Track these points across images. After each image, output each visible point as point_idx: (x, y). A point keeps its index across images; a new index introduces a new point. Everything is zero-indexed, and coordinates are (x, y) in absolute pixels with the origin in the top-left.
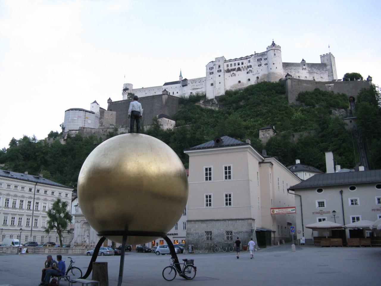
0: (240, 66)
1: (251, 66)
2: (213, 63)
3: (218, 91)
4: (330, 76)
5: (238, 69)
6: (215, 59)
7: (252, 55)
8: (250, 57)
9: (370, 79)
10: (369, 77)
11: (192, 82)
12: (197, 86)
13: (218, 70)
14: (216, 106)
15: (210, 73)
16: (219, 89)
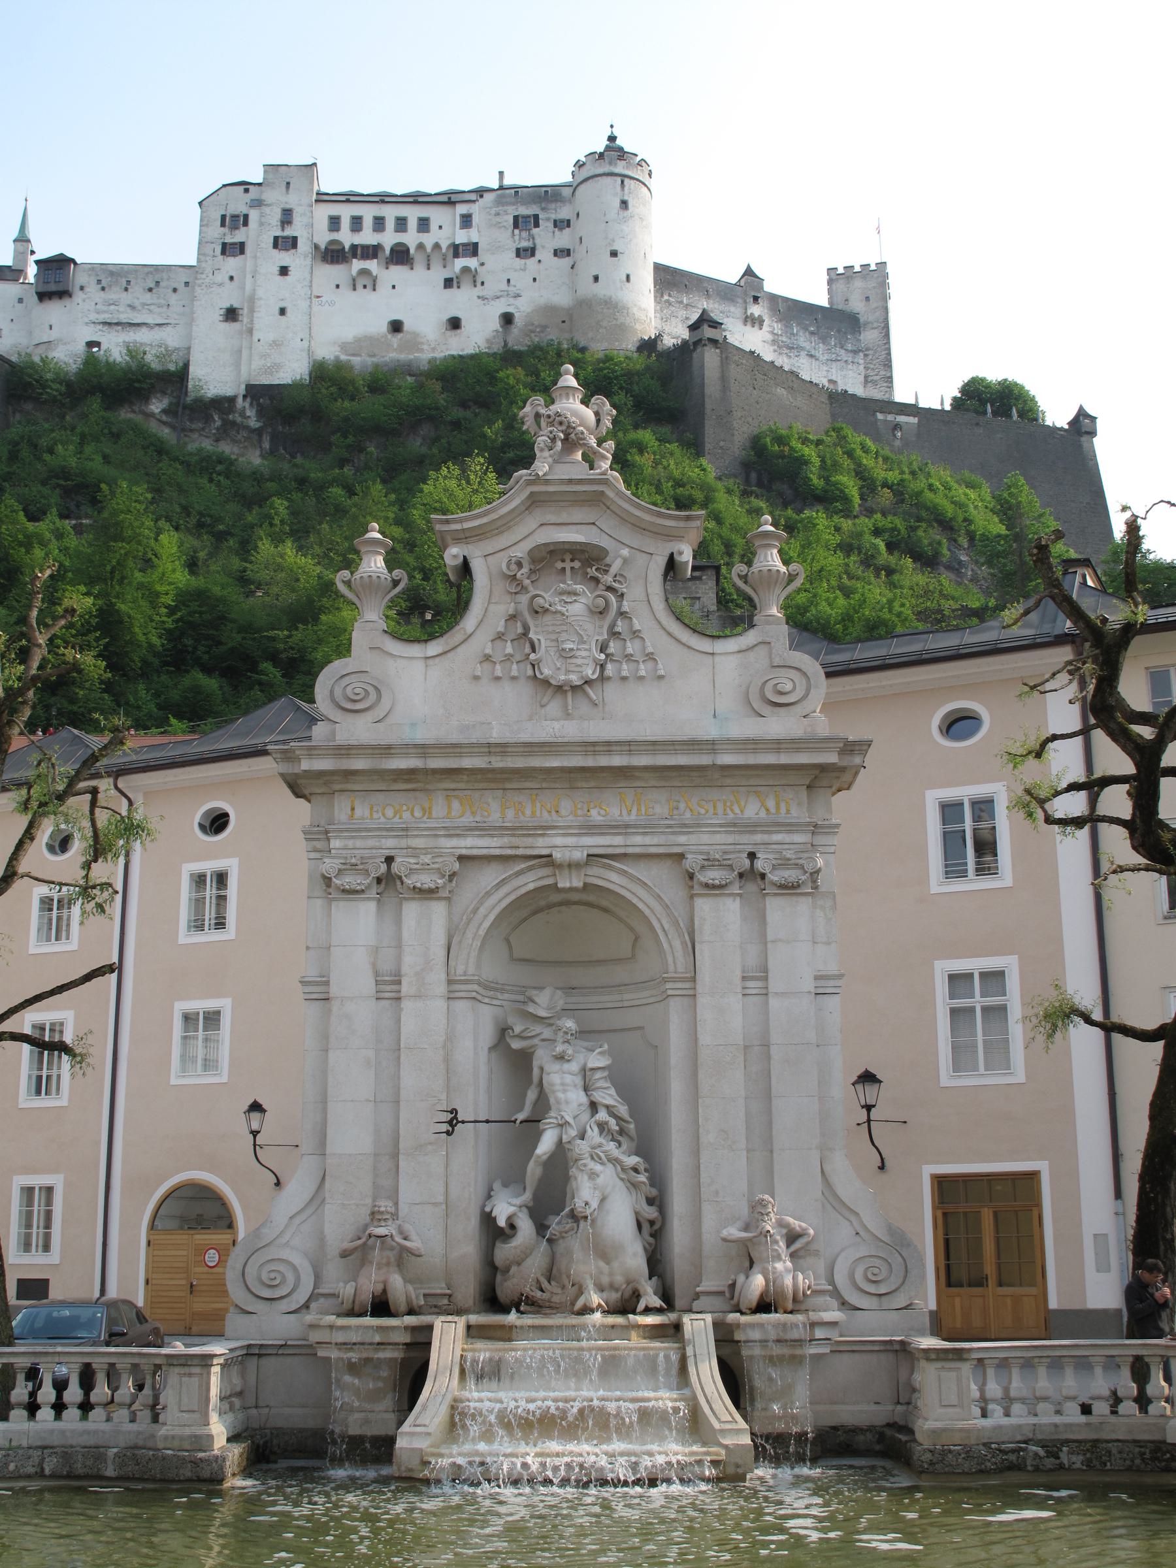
0: (411, 238)
1: (473, 249)
2: (247, 191)
3: (265, 356)
4: (875, 383)
5: (392, 250)
6: (265, 172)
7: (481, 192)
8: (473, 197)
9: (1083, 425)
10: (1082, 414)
11: (104, 283)
12: (132, 307)
13: (276, 239)
14: (247, 439)
15: (224, 245)
16: (276, 344)
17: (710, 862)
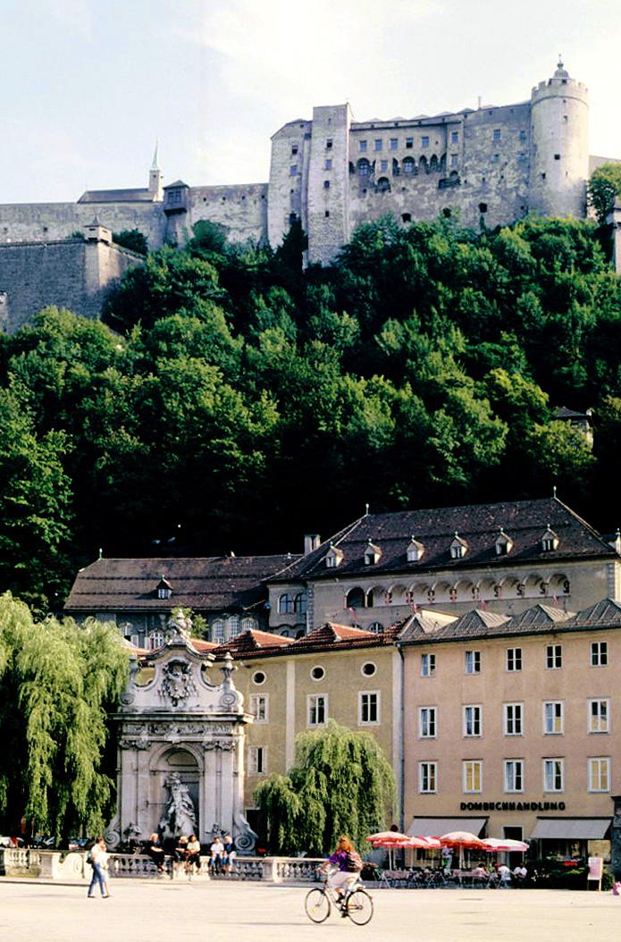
17: (209, 743)
